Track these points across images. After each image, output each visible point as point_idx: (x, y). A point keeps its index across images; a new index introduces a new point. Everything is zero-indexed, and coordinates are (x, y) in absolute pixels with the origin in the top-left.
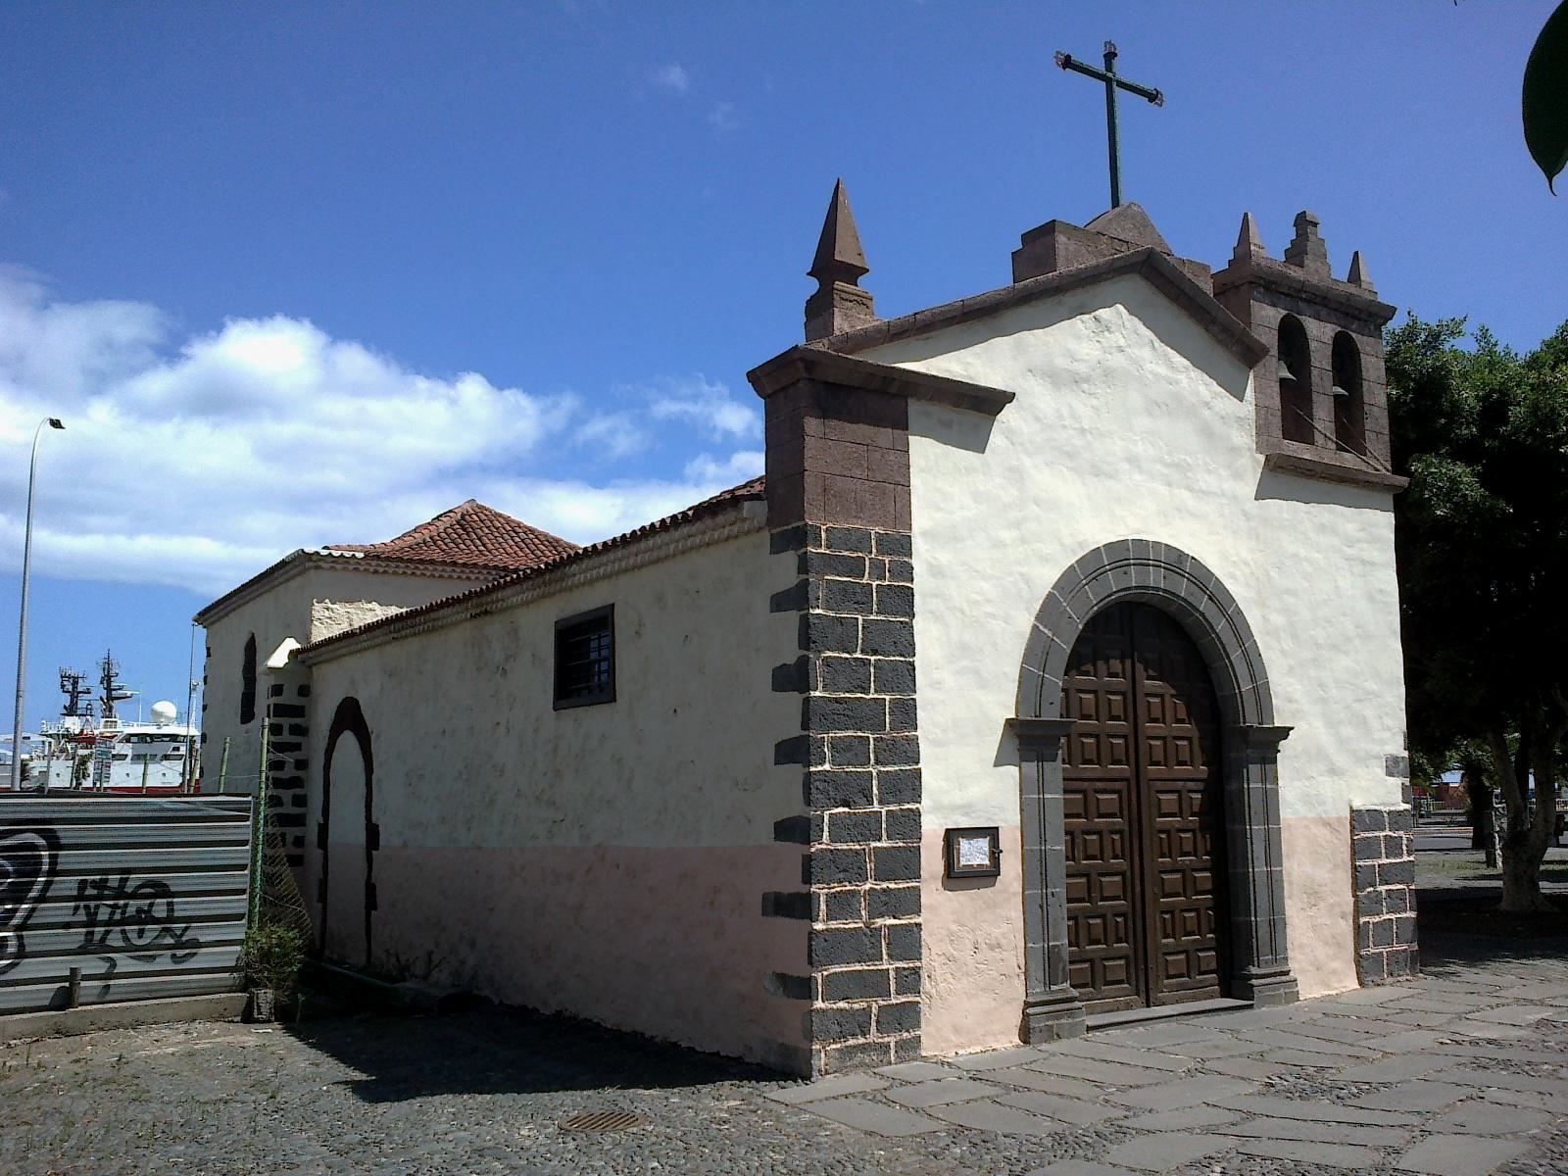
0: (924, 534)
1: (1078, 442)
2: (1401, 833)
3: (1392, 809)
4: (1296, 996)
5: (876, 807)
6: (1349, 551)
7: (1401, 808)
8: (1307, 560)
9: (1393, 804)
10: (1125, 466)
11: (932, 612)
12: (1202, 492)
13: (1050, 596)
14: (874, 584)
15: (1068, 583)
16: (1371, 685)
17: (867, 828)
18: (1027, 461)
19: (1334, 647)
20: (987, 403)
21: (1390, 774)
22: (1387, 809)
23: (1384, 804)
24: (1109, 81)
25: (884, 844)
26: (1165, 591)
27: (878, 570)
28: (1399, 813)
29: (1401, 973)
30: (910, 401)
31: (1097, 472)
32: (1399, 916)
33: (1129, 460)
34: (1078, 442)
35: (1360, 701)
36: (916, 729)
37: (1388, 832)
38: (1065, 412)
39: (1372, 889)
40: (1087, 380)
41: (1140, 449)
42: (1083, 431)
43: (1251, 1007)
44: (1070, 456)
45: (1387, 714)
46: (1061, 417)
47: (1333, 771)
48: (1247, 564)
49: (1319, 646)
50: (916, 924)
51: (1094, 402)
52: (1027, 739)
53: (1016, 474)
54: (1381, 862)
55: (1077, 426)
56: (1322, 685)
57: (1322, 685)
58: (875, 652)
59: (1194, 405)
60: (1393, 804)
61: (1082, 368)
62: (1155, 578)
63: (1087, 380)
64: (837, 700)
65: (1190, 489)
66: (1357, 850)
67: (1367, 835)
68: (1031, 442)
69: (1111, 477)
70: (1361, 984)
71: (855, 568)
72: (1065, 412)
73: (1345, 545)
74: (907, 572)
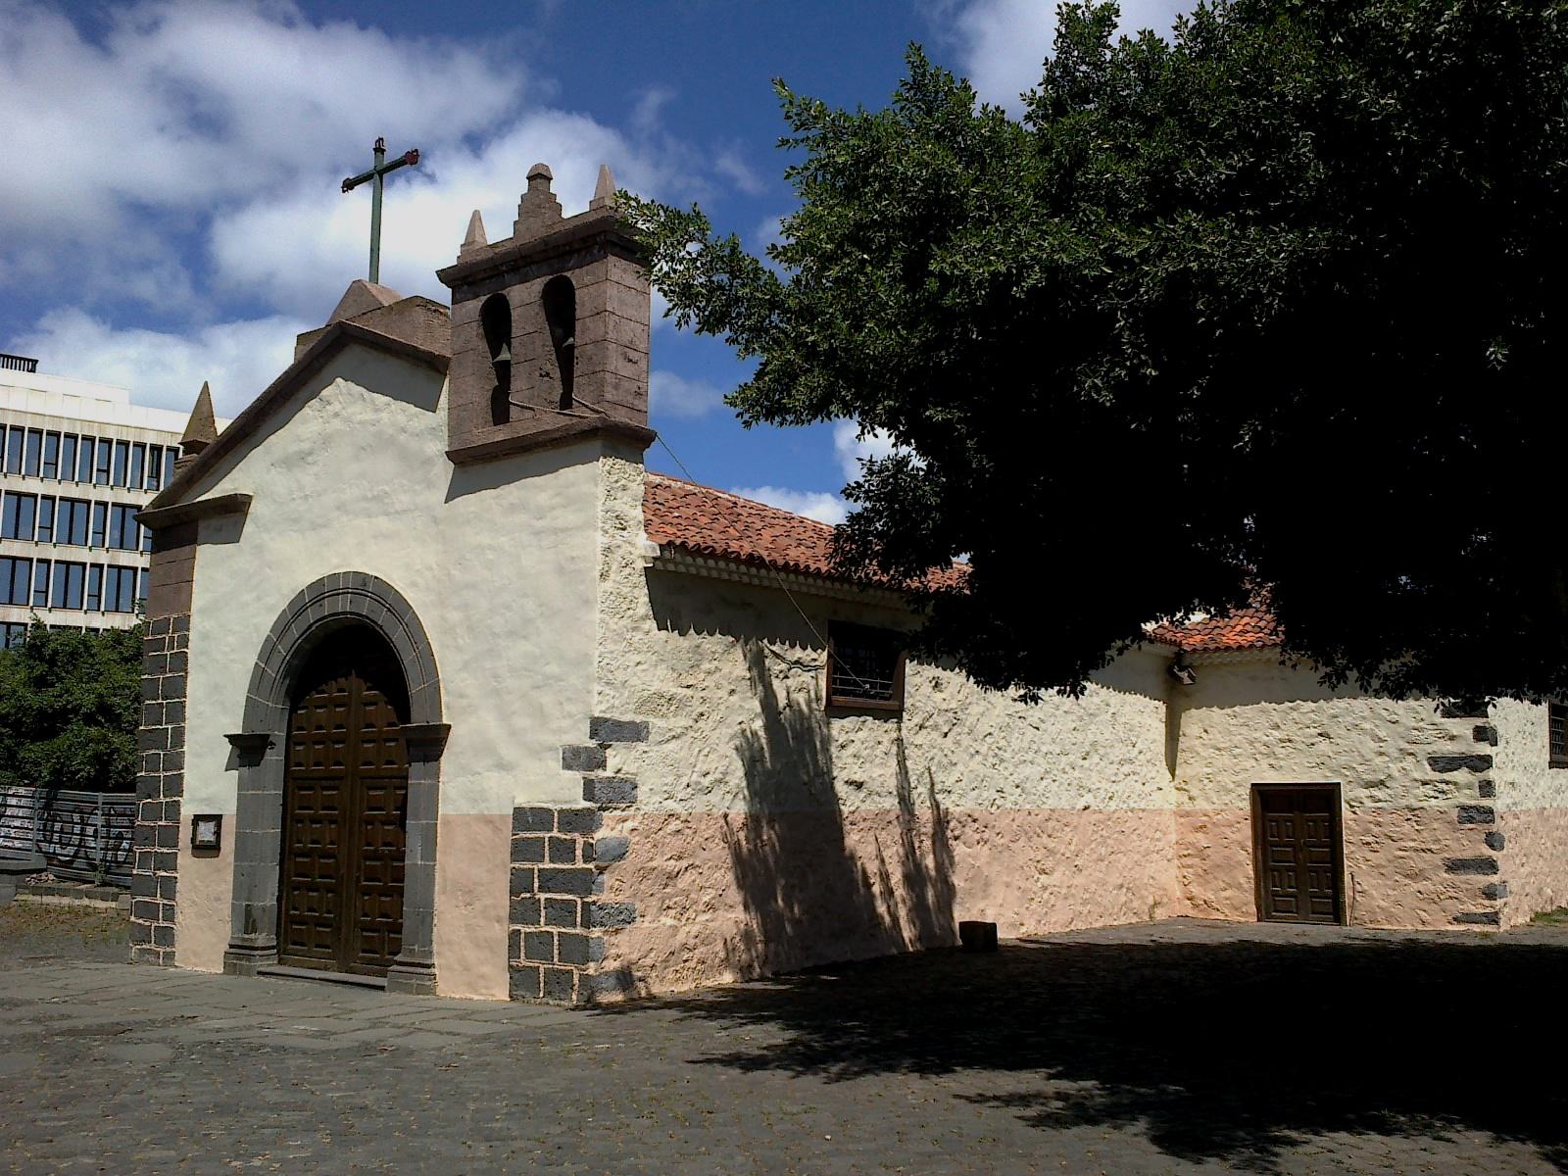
0: (202, 611)
2: (576, 835)
3: (564, 807)
4: (431, 991)
5: (162, 799)
6: (539, 524)
7: (579, 807)
8: (491, 548)
9: (566, 802)
12: (397, 512)
13: (268, 636)
15: (282, 627)
16: (553, 669)
18: (265, 536)
19: (512, 634)
21: (567, 766)
22: (558, 807)
23: (554, 801)
26: (351, 613)
28: (576, 813)
29: (562, 996)
32: (563, 930)
33: (338, 508)
35: (538, 687)
37: (555, 833)
39: (528, 895)
43: (382, 988)
44: (295, 521)
45: (569, 699)
47: (502, 766)
48: (431, 569)
49: (495, 635)
51: (315, 469)
52: (247, 749)
53: (259, 550)
54: (541, 866)
56: (496, 677)
57: (496, 677)
59: (392, 436)
60: (566, 802)
61: (306, 446)
62: (343, 604)
63: (310, 454)
64: (149, 731)
65: (387, 514)
66: (519, 850)
67: (528, 835)
69: (325, 526)
70: (511, 997)
73: (535, 518)
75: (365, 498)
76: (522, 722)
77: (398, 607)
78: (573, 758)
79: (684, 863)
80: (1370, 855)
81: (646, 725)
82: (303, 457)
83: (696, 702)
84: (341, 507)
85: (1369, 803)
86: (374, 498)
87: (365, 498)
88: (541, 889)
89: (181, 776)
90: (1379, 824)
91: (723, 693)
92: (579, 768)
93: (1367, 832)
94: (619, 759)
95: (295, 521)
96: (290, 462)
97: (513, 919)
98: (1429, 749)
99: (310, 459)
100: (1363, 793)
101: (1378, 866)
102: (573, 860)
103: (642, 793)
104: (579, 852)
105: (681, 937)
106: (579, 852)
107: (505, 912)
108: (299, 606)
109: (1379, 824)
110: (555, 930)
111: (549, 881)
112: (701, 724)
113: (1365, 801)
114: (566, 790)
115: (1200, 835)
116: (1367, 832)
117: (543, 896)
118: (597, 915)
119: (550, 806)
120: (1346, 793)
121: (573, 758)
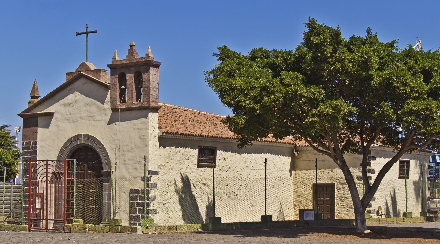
1: (70, 117)
6: (135, 127)
10: (80, 119)
13: (62, 148)
15: (66, 146)
18: (59, 123)
19: (128, 151)
24: (87, 33)
27: (32, 148)
31: (74, 122)
33: (80, 118)
34: (70, 117)
37: (140, 195)
38: (67, 111)
40: (72, 104)
41: (83, 115)
42: (71, 114)
44: (68, 120)
46: (66, 112)
49: (124, 151)
56: (125, 161)
57: (125, 161)
61: (70, 102)
62: (84, 142)
63: (72, 104)
65: (94, 121)
66: (131, 198)
72: (67, 111)
75: (88, 116)
76: (130, 170)
77: (99, 143)
79: (167, 201)
80: (341, 203)
81: (159, 172)
82: (69, 104)
83: (169, 166)
84: (81, 118)
85: (342, 189)
86: (90, 116)
87: (88, 116)
88: (137, 206)
90: (344, 194)
91: (175, 164)
93: (341, 196)
94: (154, 179)
95: (68, 120)
97: (130, 213)
98: (357, 174)
99: (71, 105)
100: (340, 186)
101: (343, 206)
103: (158, 186)
105: (166, 218)
107: (128, 212)
108: (70, 141)
109: (344, 194)
110: (141, 215)
111: (139, 205)
112: (170, 171)
113: (341, 188)
115: (300, 198)
116: (341, 196)
117: (137, 208)
118: (150, 212)
120: (336, 186)
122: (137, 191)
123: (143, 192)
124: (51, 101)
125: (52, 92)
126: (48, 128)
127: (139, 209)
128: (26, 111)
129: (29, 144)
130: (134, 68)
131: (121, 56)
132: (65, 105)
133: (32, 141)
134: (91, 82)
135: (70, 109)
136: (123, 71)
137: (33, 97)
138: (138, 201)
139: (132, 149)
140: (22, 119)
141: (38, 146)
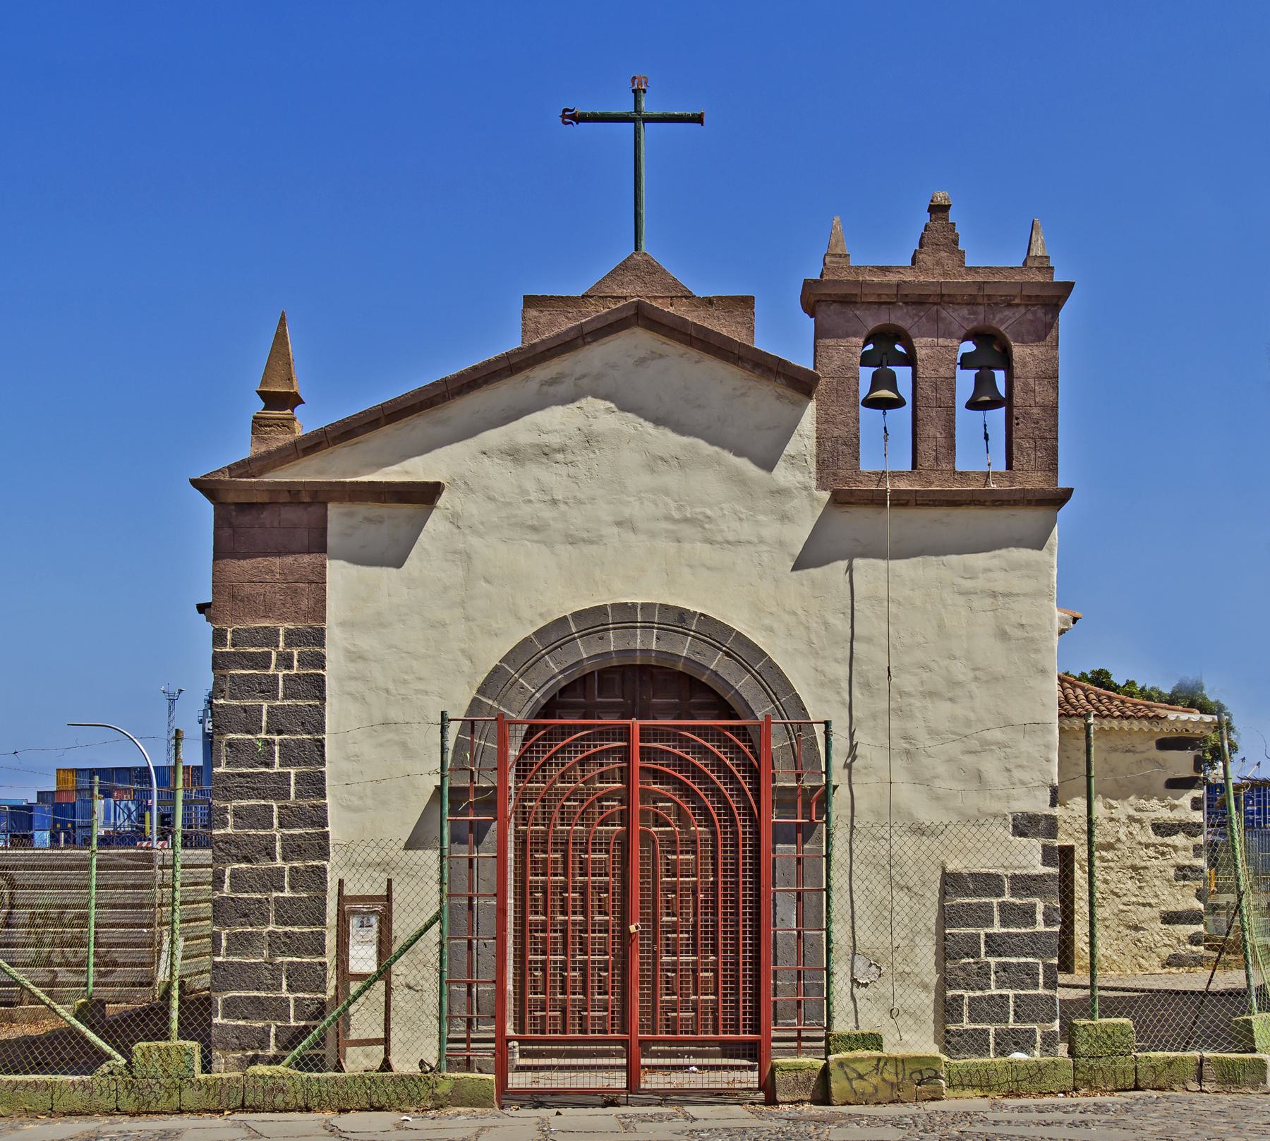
1: (547, 513)
2: (1037, 900)
5: (279, 862)
6: (968, 584)
7: (1036, 872)
10: (615, 530)
11: (350, 694)
14: (281, 674)
16: (997, 735)
17: (273, 880)
18: (474, 541)
19: (931, 694)
20: (427, 494)
21: (1019, 831)
25: (287, 893)
27: (286, 661)
28: (1035, 878)
30: (329, 506)
31: (572, 540)
33: (619, 524)
34: (547, 513)
36: (324, 797)
37: (1007, 898)
38: (531, 486)
39: (971, 960)
40: (562, 450)
41: (633, 510)
42: (554, 502)
44: (534, 529)
46: (524, 492)
50: (320, 964)
51: (571, 470)
52: (460, 811)
54: (989, 931)
55: (547, 498)
58: (280, 732)
61: (555, 440)
62: (646, 642)
63: (562, 450)
64: (240, 775)
68: (482, 523)
69: (592, 542)
71: (264, 661)
72: (531, 486)
74: (320, 661)
75: (669, 518)
76: (943, 785)
78: (1025, 826)
87: (669, 518)
89: (325, 836)
92: (1035, 835)
95: (534, 529)
96: (514, 454)
102: (1034, 923)
104: (1039, 917)
106: (1039, 917)
110: (1011, 993)
111: (995, 944)
114: (1029, 857)
117: (993, 961)
119: (1000, 871)
121: (1025, 826)
122: (989, 883)
123: (1024, 884)
124: (418, 426)
125: (445, 381)
126: (399, 564)
127: (1004, 967)
128: (243, 468)
129: (270, 637)
130: (965, 311)
131: (886, 251)
132: (514, 454)
133: (283, 627)
134: (694, 354)
135: (553, 476)
136: (899, 318)
137: (273, 400)
138: (997, 929)
139: (954, 684)
140: (206, 509)
141: (331, 653)
